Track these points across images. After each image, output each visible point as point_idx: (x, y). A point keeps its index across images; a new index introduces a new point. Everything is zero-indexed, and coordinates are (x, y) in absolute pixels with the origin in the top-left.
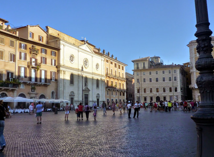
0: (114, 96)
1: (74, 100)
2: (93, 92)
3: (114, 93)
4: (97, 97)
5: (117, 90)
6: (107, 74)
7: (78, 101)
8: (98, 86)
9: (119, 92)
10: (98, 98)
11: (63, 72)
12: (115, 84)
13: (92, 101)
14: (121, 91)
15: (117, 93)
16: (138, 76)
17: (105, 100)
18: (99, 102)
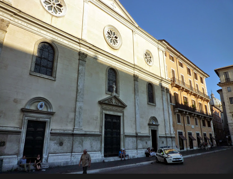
0: (193, 127)
1: (47, 132)
2: (138, 112)
3: (192, 120)
4: (149, 124)
5: (198, 116)
6: (174, 80)
7: (73, 135)
8: (151, 99)
9: (200, 119)
10: (153, 128)
12: (192, 103)
13: (135, 134)
14: (205, 117)
15: (198, 121)
16: (230, 93)
17: (172, 133)
18: (158, 138)
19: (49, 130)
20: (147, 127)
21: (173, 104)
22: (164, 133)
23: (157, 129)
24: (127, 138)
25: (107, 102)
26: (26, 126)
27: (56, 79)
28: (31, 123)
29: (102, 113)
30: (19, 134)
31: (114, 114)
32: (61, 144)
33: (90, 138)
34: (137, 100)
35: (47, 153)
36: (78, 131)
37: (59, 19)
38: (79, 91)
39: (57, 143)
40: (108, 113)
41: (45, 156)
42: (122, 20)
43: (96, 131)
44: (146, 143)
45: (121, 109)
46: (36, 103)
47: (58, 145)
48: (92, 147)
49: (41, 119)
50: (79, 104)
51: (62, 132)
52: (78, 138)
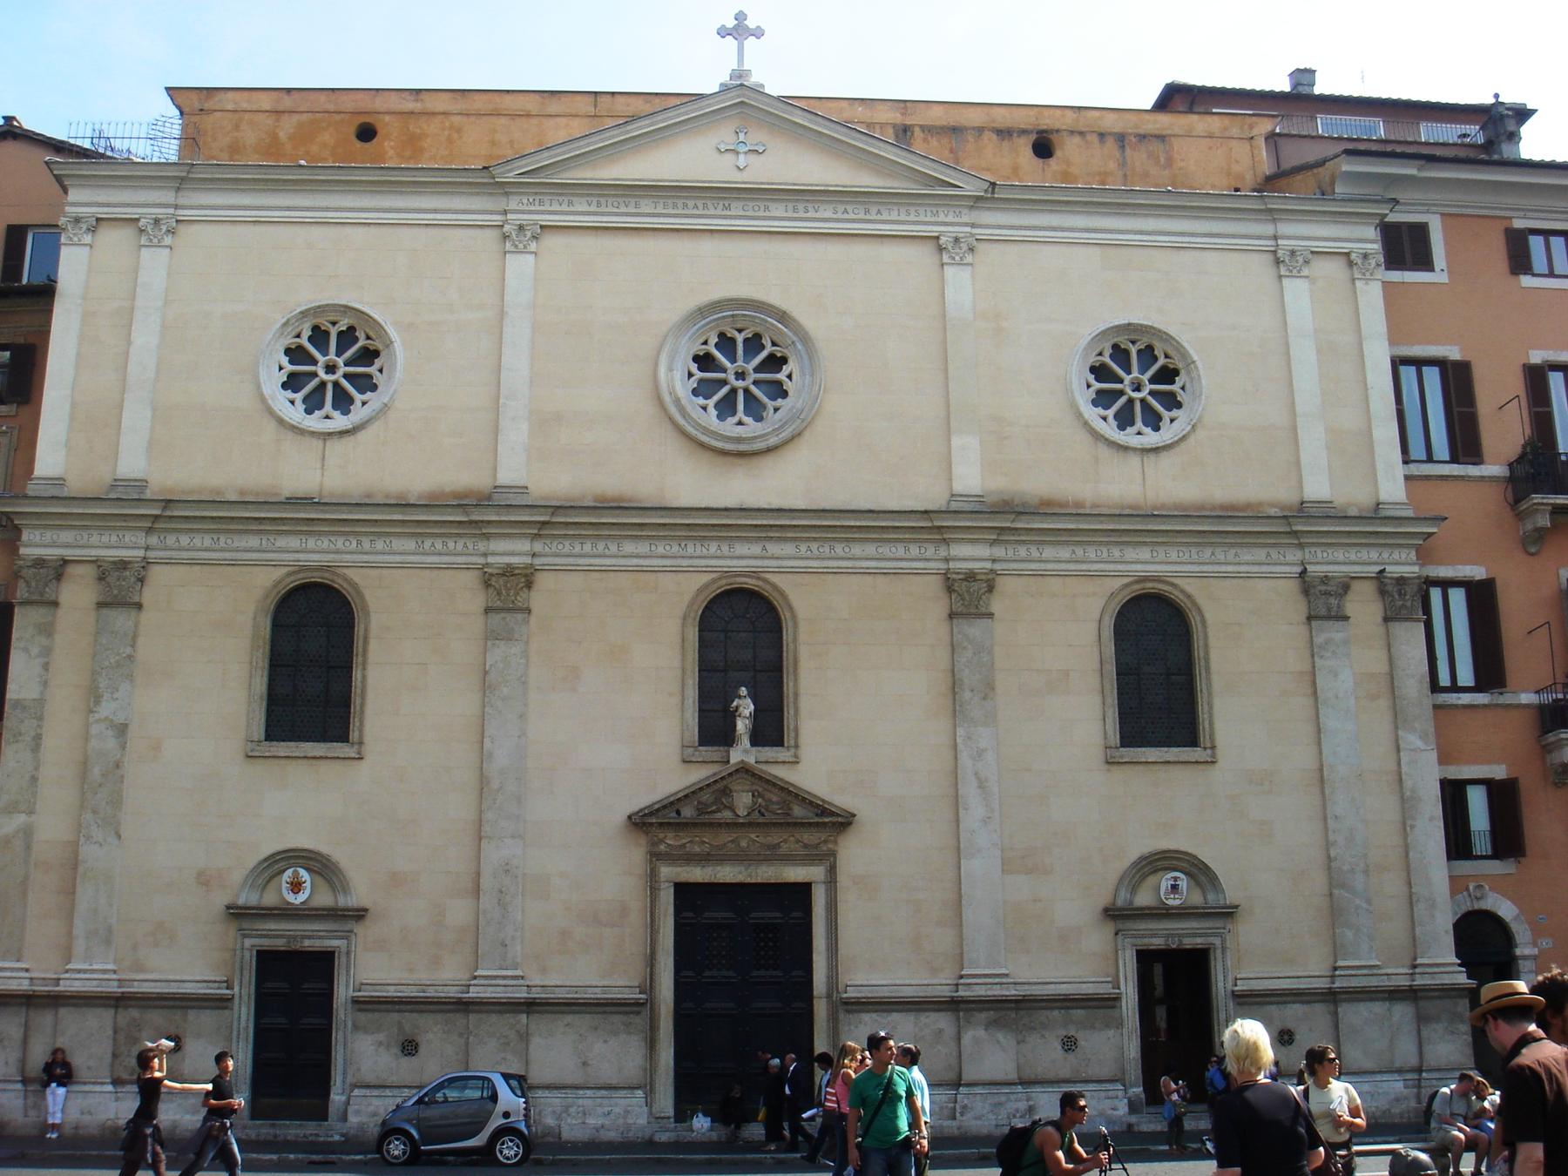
1: (343, 992)
7: (464, 1006)
11: (77, 594)
19: (347, 986)
20: (1098, 939)
21: (1527, 698)
22: (862, 978)
23: (1217, 941)
25: (688, 812)
26: (250, 976)
27: (367, 749)
28: (270, 964)
29: (652, 879)
30: (226, 1008)
31: (749, 880)
32: (410, 1048)
33: (569, 1018)
34: (980, 753)
35: (347, 1086)
36: (490, 989)
37: (362, 436)
38: (495, 785)
39: (388, 1047)
41: (336, 1098)
42: (825, 217)
43: (622, 983)
44: (1069, 1044)
45: (808, 837)
46: (273, 884)
47: (396, 1050)
48: (585, 1064)
49: (307, 943)
50: (493, 855)
52: (494, 1018)
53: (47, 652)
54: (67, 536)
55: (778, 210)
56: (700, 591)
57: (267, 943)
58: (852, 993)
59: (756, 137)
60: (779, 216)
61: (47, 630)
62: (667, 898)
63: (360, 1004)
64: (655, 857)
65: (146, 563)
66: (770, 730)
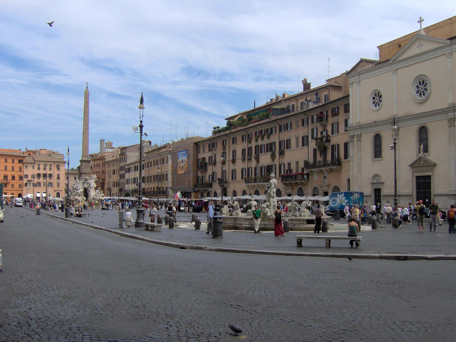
24: (437, 197)
29: (413, 175)
33: (404, 197)
40: (418, 175)
45: (431, 168)
51: (388, 194)
53: (353, 148)
54: (353, 132)
55: (425, 56)
56: (418, 127)
57: (376, 188)
58: (436, 193)
59: (422, 42)
60: (425, 57)
61: (353, 145)
62: (415, 178)
63: (384, 196)
64: (413, 172)
65: (361, 134)
66: (426, 150)
